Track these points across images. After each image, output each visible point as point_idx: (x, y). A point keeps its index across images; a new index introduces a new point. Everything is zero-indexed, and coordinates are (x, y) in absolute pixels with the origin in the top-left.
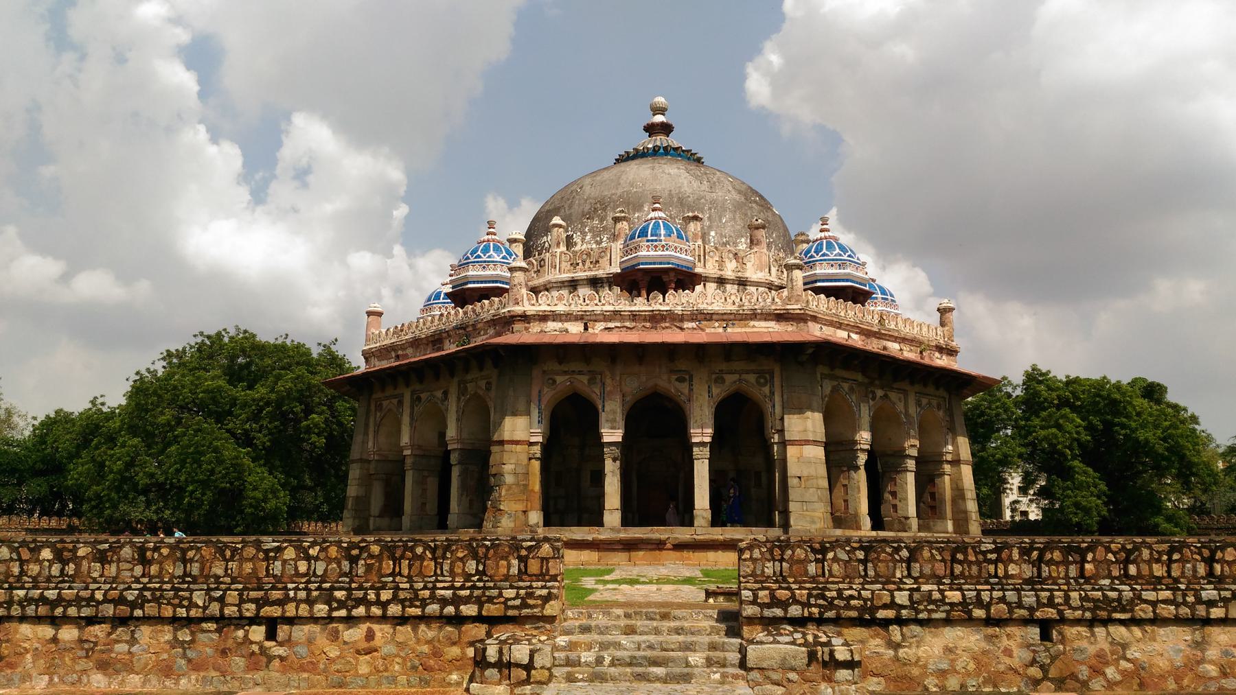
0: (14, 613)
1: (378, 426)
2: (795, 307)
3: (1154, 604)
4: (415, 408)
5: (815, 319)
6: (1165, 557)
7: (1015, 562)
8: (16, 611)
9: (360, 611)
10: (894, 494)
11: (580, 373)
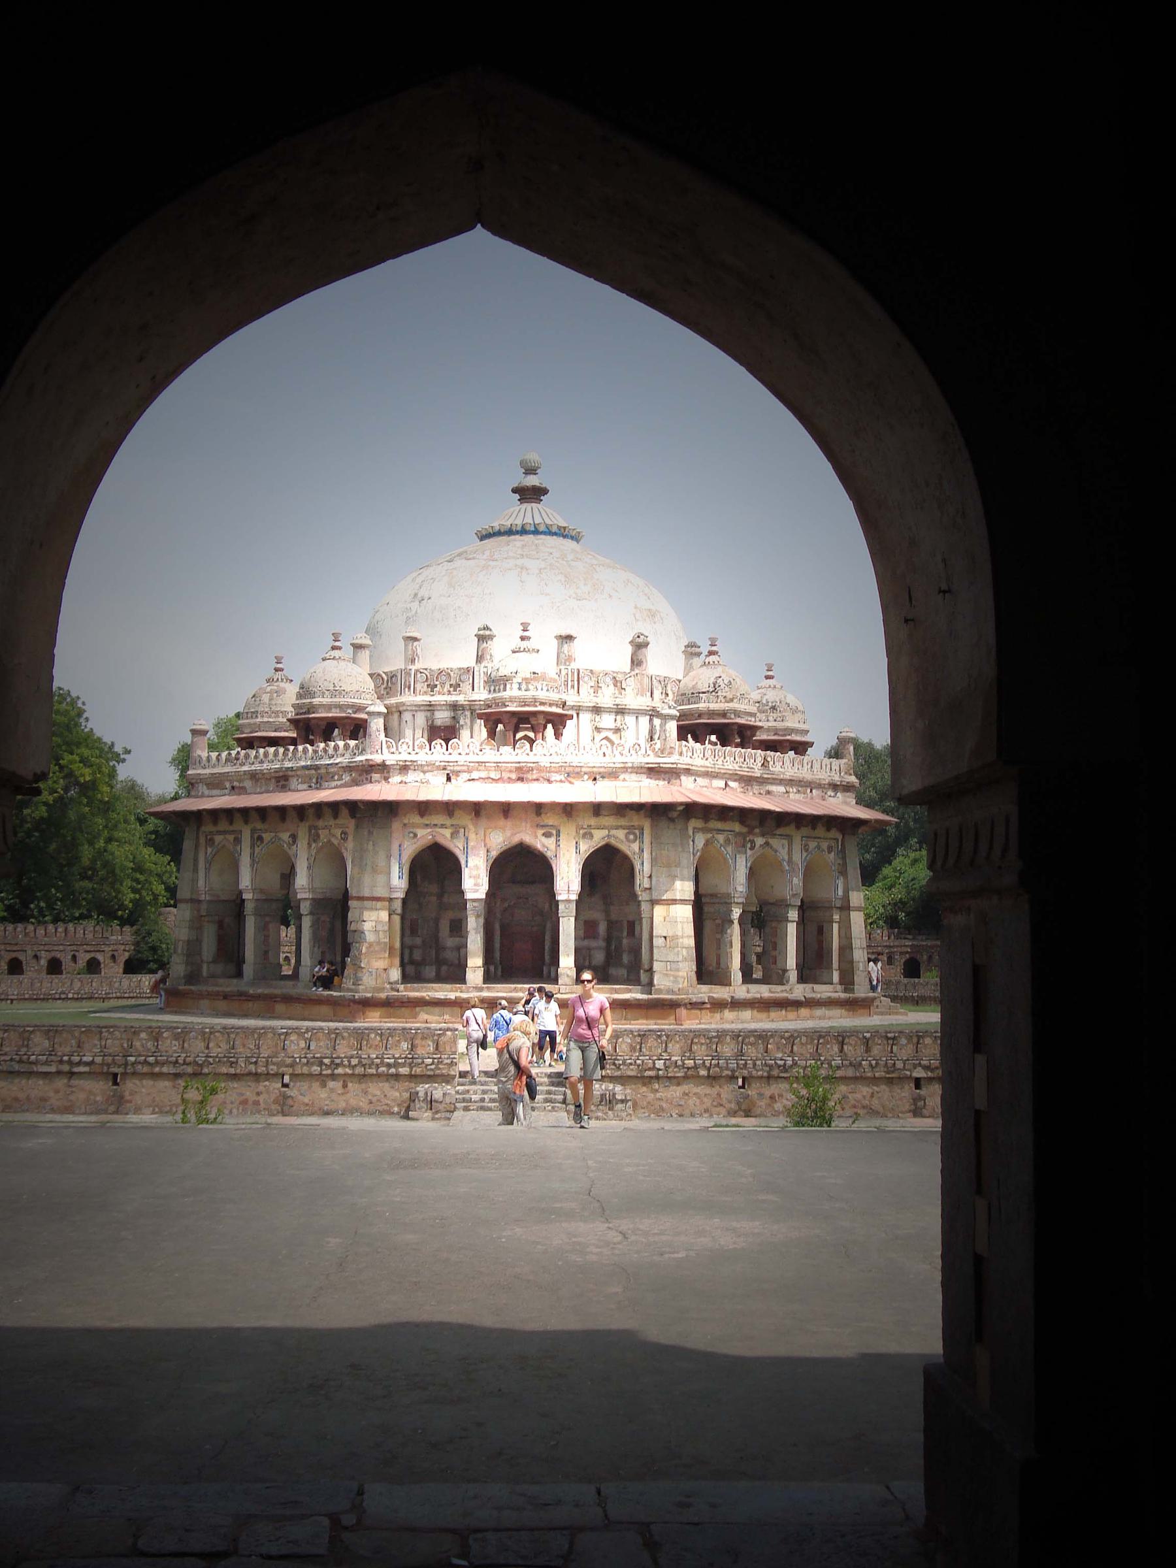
0: (128, 1071)
2: (666, 761)
3: (805, 1068)
4: (256, 849)
5: (688, 772)
6: (816, 1041)
7: (728, 1044)
8: (130, 1069)
9: (340, 1071)
11: (443, 826)
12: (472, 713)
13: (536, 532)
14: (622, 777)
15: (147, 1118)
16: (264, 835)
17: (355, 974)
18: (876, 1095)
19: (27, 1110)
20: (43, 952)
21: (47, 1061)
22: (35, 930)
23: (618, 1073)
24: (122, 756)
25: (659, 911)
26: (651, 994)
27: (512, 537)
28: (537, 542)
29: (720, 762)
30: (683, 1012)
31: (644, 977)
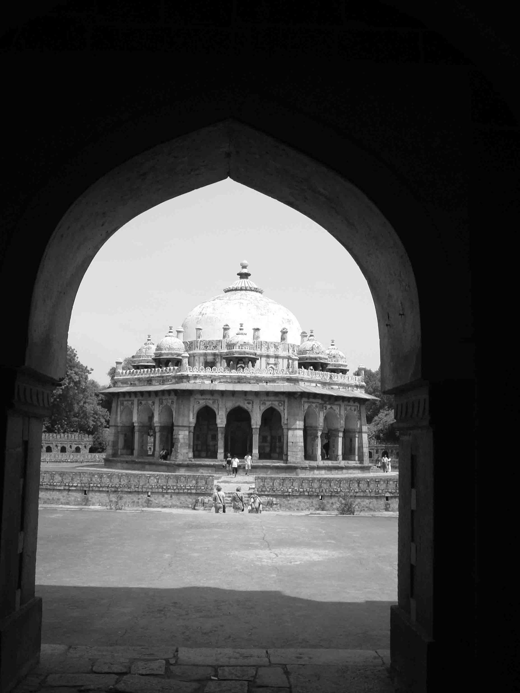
1: (122, 412)
6: (349, 482)
7: (316, 483)
8: (91, 489)
9: (169, 491)
10: (334, 446)
11: (209, 399)
12: (221, 357)
13: (246, 290)
14: (277, 382)
15: (97, 507)
16: (142, 402)
17: (176, 455)
18: (371, 503)
19: (52, 503)
20: (59, 444)
21: (60, 485)
22: (56, 435)
23: (274, 494)
24: (90, 371)
25: (290, 433)
26: (287, 464)
27: (237, 292)
28: (246, 293)
29: (314, 376)
30: (299, 471)
31: (284, 457)
